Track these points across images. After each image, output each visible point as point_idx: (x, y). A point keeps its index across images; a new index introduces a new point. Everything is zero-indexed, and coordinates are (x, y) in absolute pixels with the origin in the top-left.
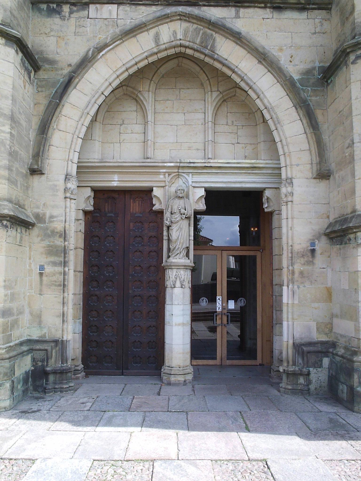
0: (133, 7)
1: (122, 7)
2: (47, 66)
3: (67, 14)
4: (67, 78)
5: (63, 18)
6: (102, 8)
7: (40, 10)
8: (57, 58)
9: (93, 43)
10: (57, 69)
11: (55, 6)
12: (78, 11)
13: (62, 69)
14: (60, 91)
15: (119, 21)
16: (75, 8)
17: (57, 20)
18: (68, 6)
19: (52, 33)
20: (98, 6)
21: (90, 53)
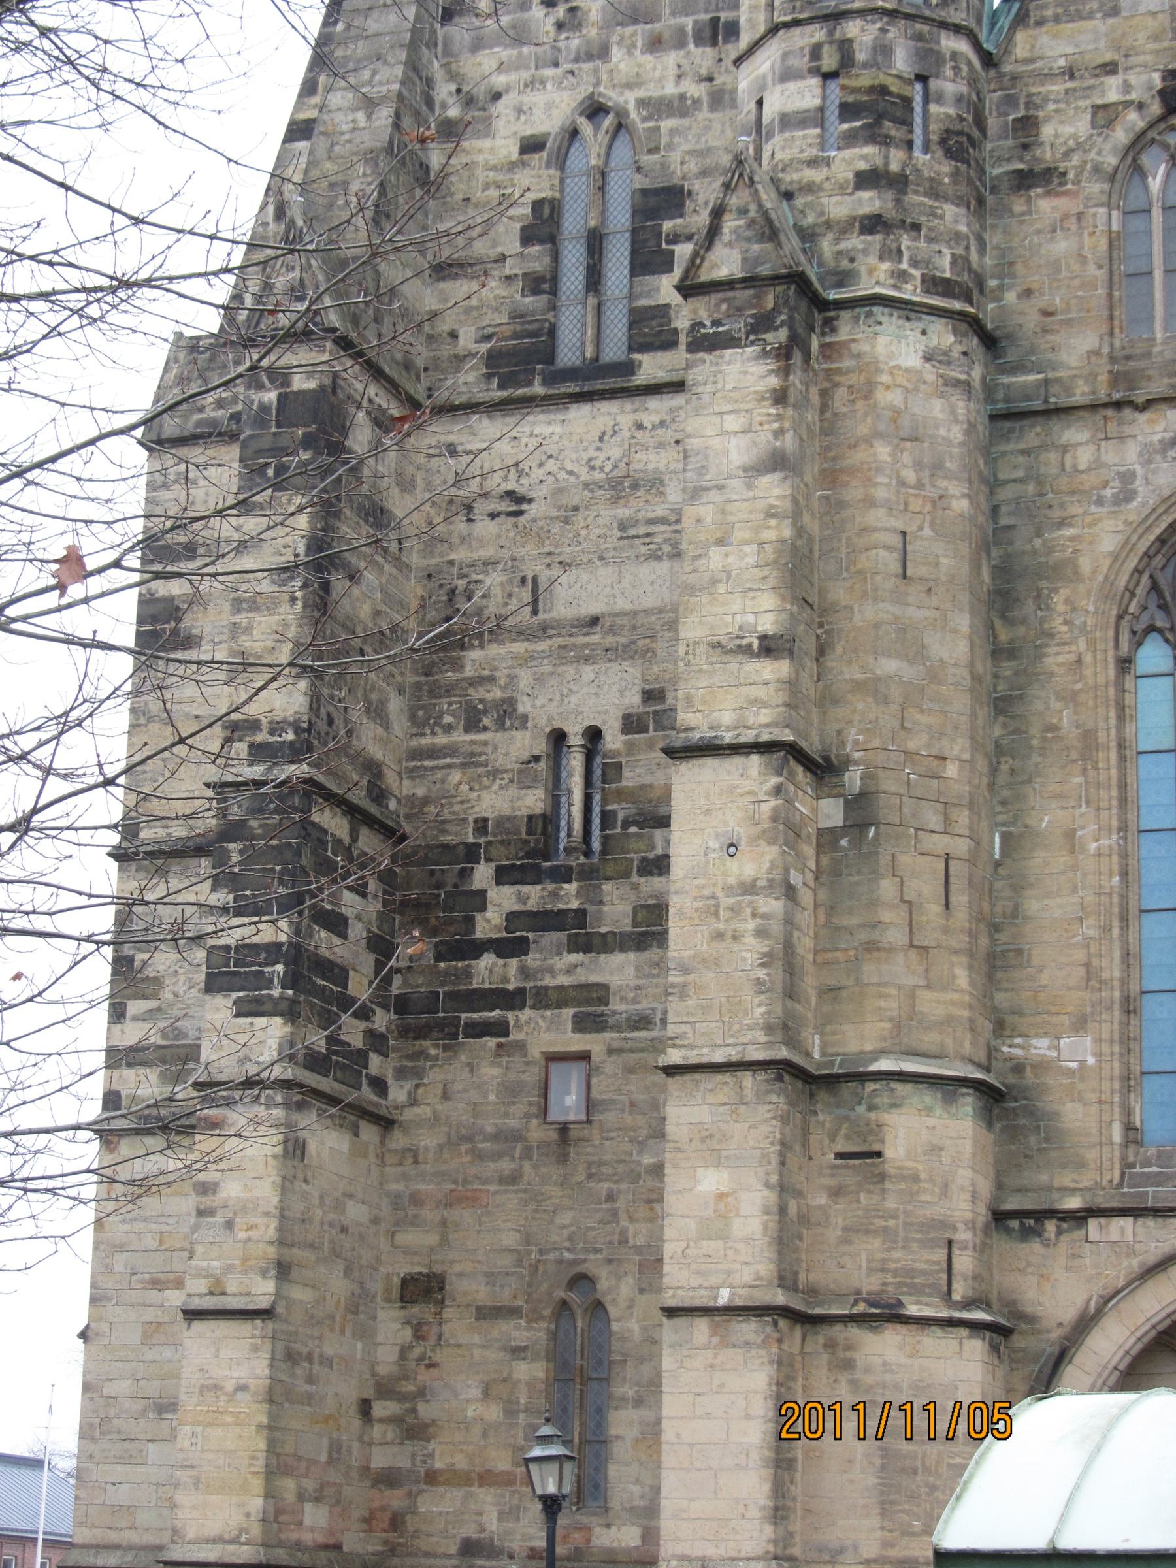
0: (1160, 1220)
1: (1140, 1222)
2: (1024, 1326)
3: (1053, 1236)
4: (1056, 1350)
5: (1046, 1244)
6: (1108, 1225)
7: (1008, 1231)
8: (1039, 1311)
9: (1097, 1289)
10: (1040, 1332)
11: (1032, 1222)
12: (1068, 1231)
13: (1048, 1331)
14: (1047, 1370)
15: (1137, 1246)
16: (1065, 1225)
17: (1036, 1246)
18: (1054, 1221)
19: (1030, 1270)
20: (1103, 1220)
21: (1093, 1304)
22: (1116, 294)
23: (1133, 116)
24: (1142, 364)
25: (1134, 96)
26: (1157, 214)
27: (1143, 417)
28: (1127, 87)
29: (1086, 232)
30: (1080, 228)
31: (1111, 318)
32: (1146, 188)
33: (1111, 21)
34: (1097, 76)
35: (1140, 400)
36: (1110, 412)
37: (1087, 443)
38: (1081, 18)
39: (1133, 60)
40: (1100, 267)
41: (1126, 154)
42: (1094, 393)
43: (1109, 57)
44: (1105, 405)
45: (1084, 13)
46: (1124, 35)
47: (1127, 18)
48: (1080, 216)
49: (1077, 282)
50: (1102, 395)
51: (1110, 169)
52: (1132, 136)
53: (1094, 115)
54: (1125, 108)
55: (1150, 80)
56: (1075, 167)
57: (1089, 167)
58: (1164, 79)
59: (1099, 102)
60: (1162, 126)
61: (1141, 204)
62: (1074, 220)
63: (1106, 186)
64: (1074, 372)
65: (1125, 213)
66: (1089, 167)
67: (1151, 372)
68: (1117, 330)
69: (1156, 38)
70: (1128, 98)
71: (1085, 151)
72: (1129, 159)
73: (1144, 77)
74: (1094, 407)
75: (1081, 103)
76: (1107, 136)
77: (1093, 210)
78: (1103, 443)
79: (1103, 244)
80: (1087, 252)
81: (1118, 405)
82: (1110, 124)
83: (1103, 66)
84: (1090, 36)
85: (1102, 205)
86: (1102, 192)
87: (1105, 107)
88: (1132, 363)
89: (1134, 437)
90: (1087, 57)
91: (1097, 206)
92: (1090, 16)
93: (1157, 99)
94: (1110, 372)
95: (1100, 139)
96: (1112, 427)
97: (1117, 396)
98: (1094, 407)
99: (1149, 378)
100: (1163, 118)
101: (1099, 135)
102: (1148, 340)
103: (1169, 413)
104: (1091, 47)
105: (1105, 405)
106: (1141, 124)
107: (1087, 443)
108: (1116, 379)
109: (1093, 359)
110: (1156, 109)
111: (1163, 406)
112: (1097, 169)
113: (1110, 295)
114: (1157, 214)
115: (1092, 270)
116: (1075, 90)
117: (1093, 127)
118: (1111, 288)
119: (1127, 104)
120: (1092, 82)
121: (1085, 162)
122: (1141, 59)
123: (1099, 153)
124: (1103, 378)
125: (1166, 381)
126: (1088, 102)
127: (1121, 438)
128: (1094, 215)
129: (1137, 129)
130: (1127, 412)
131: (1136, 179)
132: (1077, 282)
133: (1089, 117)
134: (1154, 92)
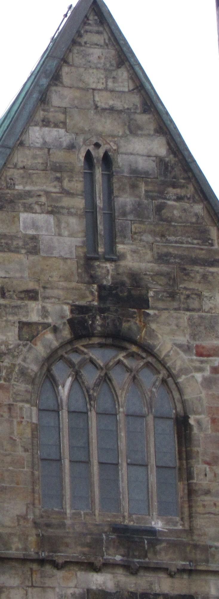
22: (36, 473)
23: (49, 336)
24: (59, 532)
25: (50, 320)
26: (64, 414)
27: (60, 574)
28: (45, 313)
29: (15, 423)
30: (11, 416)
31: (33, 492)
32: (56, 394)
33: (32, 258)
34: (22, 299)
35: (61, 561)
36: (35, 566)
37: (18, 587)
38: (10, 251)
39: (49, 292)
40: (26, 450)
41: (43, 364)
42: (25, 549)
43: (31, 285)
44: (33, 561)
45: (12, 248)
46: (42, 270)
47: (44, 258)
48: (10, 407)
49: (8, 459)
50: (32, 551)
51: (32, 374)
52: (49, 351)
53: (20, 329)
54: (44, 328)
55: (62, 310)
56: (6, 367)
57: (17, 369)
58: (72, 312)
59: (24, 320)
60: (69, 348)
61: (51, 404)
62: (6, 409)
63: (29, 387)
64: (8, 531)
65: (39, 410)
66: (17, 369)
67: (68, 540)
68: (37, 502)
69: (67, 278)
70: (46, 321)
71: (14, 357)
72: (45, 369)
73: (58, 307)
74: (24, 561)
75: (10, 318)
76: (30, 348)
77: (20, 404)
78: (30, 590)
79: (28, 431)
80: (15, 436)
81: (42, 562)
82: (32, 338)
83: (27, 292)
84: (17, 267)
85: (27, 401)
86: (26, 391)
87: (29, 324)
88: (50, 530)
89: (53, 588)
90: (15, 282)
91: (22, 401)
92: (17, 250)
93: (68, 326)
94: (38, 535)
95: (25, 350)
96: (36, 577)
97: (43, 555)
98: (24, 561)
99: (67, 545)
100: (70, 342)
101: (25, 345)
102: (59, 513)
103: (79, 573)
104: (18, 275)
105: (33, 561)
106: (56, 344)
107: (18, 587)
108: (42, 541)
109: (22, 522)
110: (66, 333)
111: (76, 568)
112: (23, 372)
113: (33, 473)
114: (64, 414)
115: (20, 451)
116: (5, 306)
117: (20, 339)
118: (33, 468)
119: (46, 326)
120: (19, 302)
121: (14, 365)
122: (56, 292)
123: (24, 360)
124: (32, 539)
125: (79, 549)
126: (16, 318)
127: (44, 588)
128: (21, 409)
129: (53, 347)
130: (48, 568)
131: (48, 384)
132: (8, 459)
133: (17, 330)
134: (65, 320)
